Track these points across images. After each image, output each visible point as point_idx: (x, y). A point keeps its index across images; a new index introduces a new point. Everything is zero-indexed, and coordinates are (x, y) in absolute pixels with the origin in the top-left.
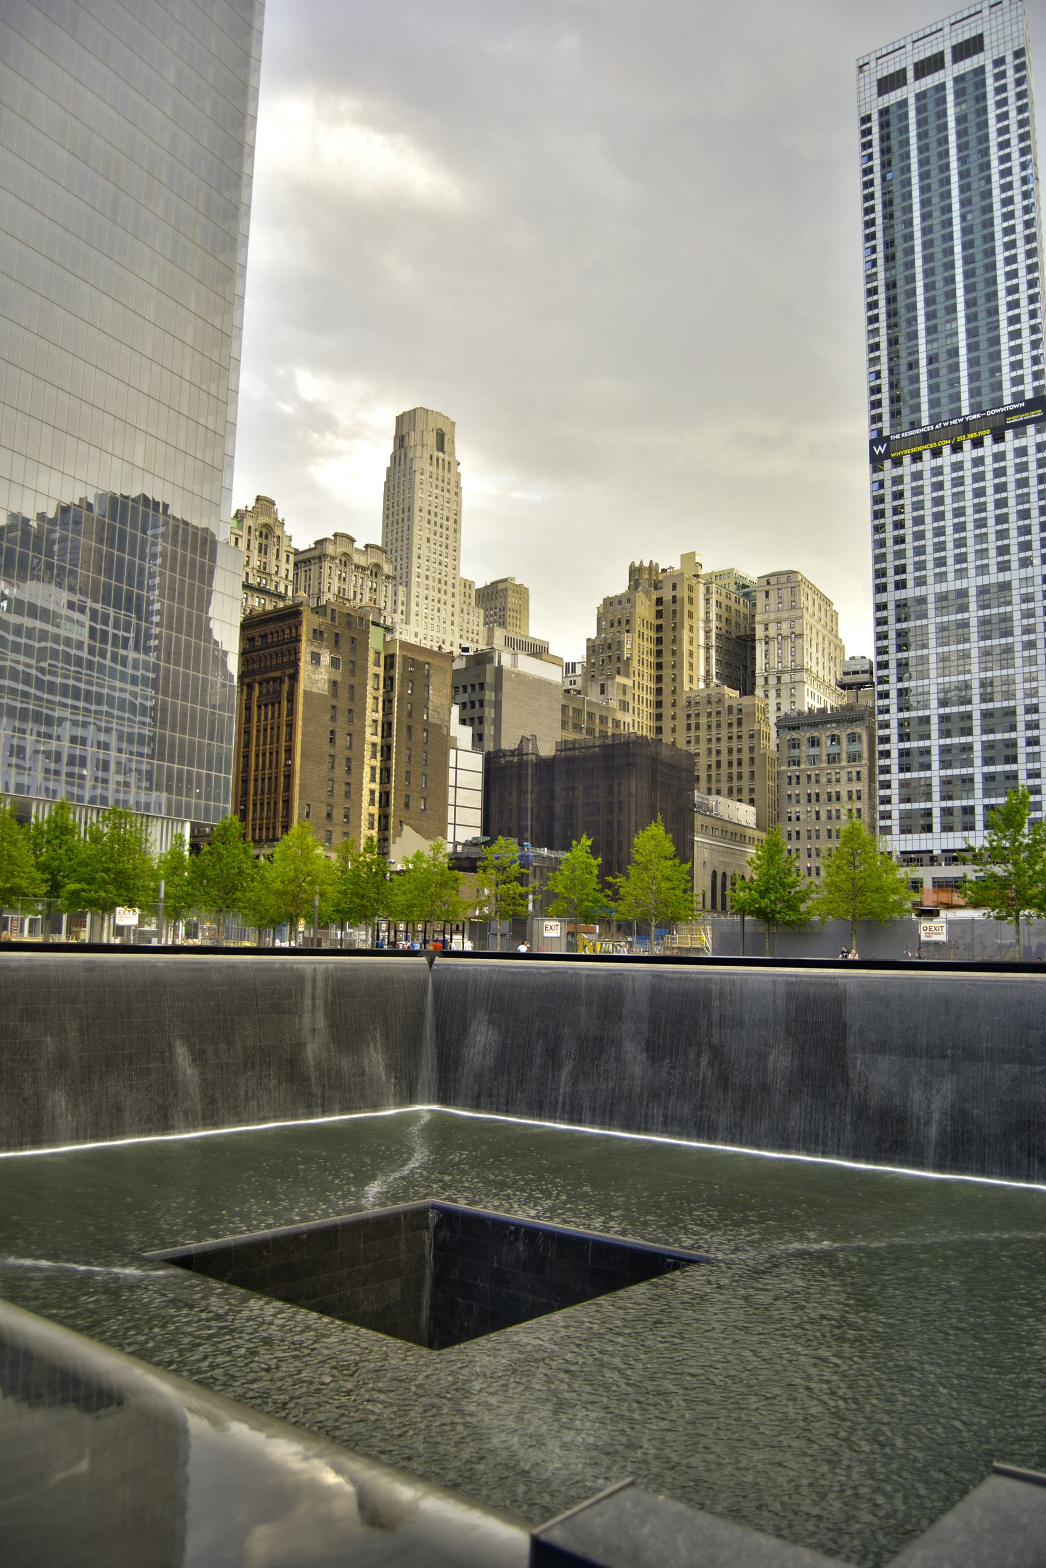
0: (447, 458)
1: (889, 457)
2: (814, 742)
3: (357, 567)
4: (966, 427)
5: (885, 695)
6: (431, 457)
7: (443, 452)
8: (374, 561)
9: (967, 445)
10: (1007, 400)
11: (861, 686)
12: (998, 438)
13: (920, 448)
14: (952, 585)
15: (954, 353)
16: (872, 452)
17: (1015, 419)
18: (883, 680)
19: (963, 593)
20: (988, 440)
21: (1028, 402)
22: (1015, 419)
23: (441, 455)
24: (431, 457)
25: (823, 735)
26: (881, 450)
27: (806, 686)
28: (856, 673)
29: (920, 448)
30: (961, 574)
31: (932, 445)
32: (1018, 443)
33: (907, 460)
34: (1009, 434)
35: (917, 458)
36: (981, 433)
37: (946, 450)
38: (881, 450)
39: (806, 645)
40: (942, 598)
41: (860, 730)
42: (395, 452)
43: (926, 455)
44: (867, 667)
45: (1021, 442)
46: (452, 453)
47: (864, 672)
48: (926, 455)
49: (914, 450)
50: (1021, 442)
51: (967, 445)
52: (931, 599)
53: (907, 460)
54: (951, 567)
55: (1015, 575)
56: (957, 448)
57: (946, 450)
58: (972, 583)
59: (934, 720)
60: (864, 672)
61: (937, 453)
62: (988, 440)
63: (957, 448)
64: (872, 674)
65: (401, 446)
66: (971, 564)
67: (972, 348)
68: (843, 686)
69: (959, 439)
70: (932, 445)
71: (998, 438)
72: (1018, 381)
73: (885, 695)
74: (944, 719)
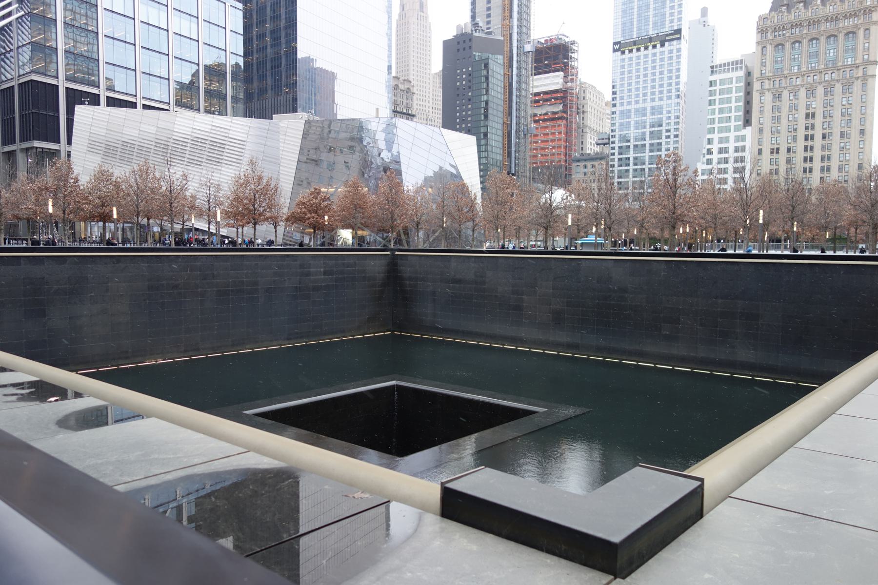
0: (425, 15)
1: (620, 50)
2: (585, 167)
3: (401, 90)
4: (650, 40)
5: (613, 148)
6: (418, 15)
7: (423, 12)
8: (408, 87)
9: (650, 47)
11: (604, 144)
13: (632, 48)
14: (641, 105)
16: (614, 48)
18: (613, 143)
19: (645, 109)
20: (658, 46)
21: (675, 30)
23: (422, 14)
24: (418, 15)
25: (589, 164)
26: (617, 47)
27: (588, 134)
28: (603, 139)
29: (632, 48)
30: (645, 101)
31: (637, 46)
32: (670, 48)
33: (627, 52)
34: (667, 44)
35: (631, 51)
36: (656, 43)
37: (642, 49)
38: (617, 47)
39: (589, 116)
40: (637, 110)
41: (603, 162)
42: (400, 13)
43: (635, 50)
44: (607, 137)
45: (671, 48)
46: (427, 14)
47: (606, 139)
48: (635, 50)
49: (630, 48)
50: (671, 48)
51: (650, 47)
52: (633, 111)
53: (627, 52)
54: (641, 98)
55: (665, 102)
56: (646, 48)
57: (642, 49)
59: (631, 159)
60: (606, 139)
61: (638, 50)
63: (646, 48)
64: (609, 139)
65: (403, 9)
66: (649, 97)
68: (598, 144)
69: (647, 44)
70: (637, 46)
71: (662, 45)
72: (672, 21)
73: (613, 148)
74: (651, 145)
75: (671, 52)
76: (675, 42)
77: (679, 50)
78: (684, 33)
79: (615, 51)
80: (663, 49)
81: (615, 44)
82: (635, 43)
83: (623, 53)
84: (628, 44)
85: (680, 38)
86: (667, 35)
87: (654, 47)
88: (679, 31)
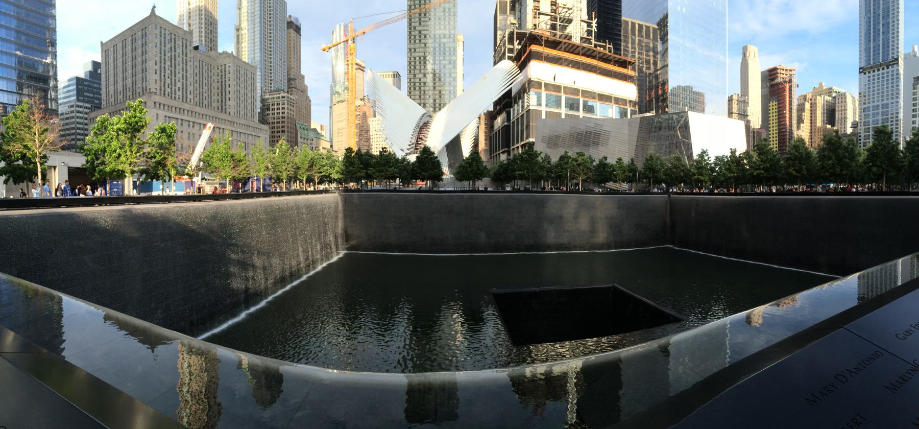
4: (881, 65)
9: (881, 69)
10: (890, 58)
12: (888, 68)
15: (879, 46)
17: (891, 63)
20: (885, 68)
22: (891, 63)
26: (861, 70)
33: (867, 73)
34: (890, 67)
35: (869, 72)
37: (876, 71)
38: (861, 70)
43: (872, 72)
45: (893, 69)
48: (872, 72)
51: (881, 69)
53: (867, 73)
56: (878, 70)
57: (876, 71)
58: (880, 103)
61: (874, 71)
62: (885, 68)
63: (878, 70)
67: (883, 45)
71: (888, 68)
75: (893, 71)
76: (895, 66)
77: (898, 70)
78: (901, 61)
79: (860, 73)
80: (888, 70)
81: (860, 68)
82: (872, 68)
83: (865, 74)
84: (867, 69)
85: (898, 63)
86: (890, 62)
87: (883, 69)
88: (897, 59)
